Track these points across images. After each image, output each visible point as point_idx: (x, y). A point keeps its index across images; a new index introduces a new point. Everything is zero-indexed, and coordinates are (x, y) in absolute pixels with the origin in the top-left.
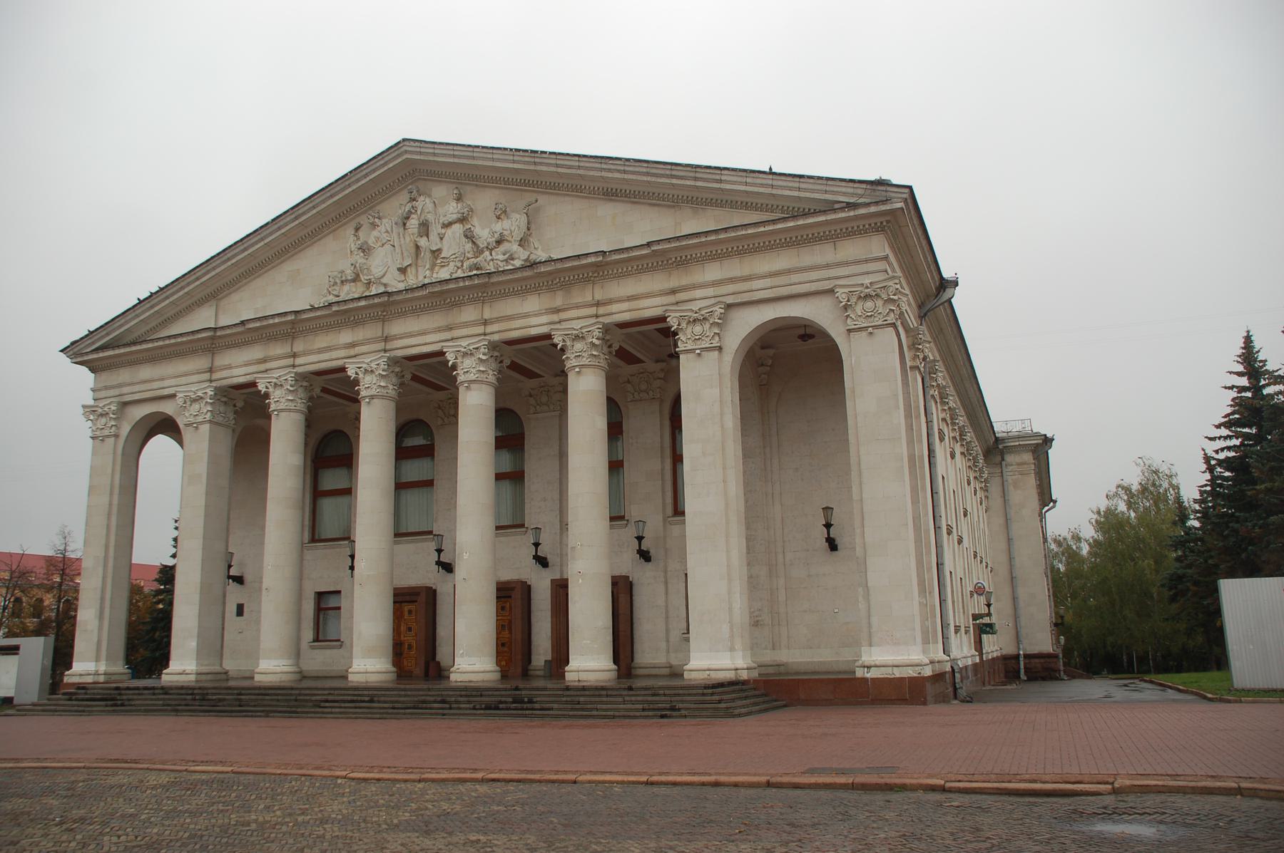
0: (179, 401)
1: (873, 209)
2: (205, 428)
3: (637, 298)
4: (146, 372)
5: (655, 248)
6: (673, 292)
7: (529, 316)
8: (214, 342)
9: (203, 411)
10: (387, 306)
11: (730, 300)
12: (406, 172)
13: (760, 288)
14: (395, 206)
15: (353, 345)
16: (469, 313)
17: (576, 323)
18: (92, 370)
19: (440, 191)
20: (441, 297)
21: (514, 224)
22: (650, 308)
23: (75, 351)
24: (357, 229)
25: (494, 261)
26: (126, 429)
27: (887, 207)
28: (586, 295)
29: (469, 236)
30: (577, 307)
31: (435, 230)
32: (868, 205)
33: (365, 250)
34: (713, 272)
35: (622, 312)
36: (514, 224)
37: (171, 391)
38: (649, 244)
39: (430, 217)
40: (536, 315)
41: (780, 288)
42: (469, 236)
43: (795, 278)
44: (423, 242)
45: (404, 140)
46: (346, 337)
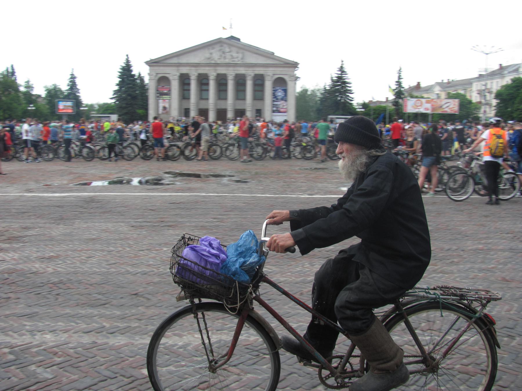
3: (260, 71)
4: (162, 68)
7: (242, 71)
8: (179, 65)
9: (177, 77)
10: (217, 65)
12: (219, 42)
13: (278, 72)
14: (217, 47)
16: (231, 69)
17: (250, 73)
18: (150, 66)
19: (225, 45)
20: (228, 65)
21: (240, 55)
22: (261, 73)
23: (147, 63)
25: (236, 61)
26: (157, 78)
28: (251, 69)
33: (211, 54)
34: (271, 69)
35: (257, 72)
36: (240, 55)
41: (280, 72)
42: (232, 56)
46: (207, 68)
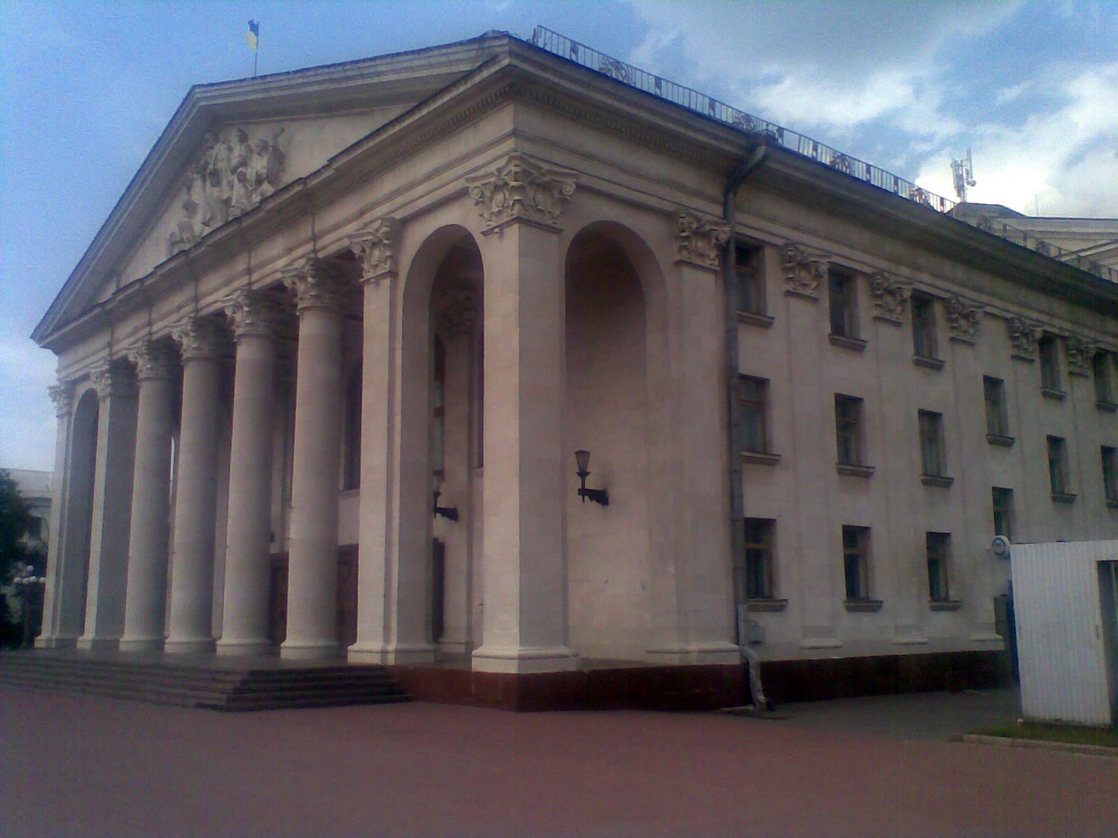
0: (93, 378)
1: (485, 74)
2: (108, 401)
3: (340, 226)
5: (335, 166)
6: (362, 213)
11: (398, 216)
13: (422, 196)
15: (179, 308)
18: (57, 352)
24: (189, 188)
27: (494, 69)
29: (243, 179)
30: (300, 245)
31: (226, 177)
32: (480, 69)
37: (87, 370)
38: (332, 161)
39: (222, 165)
40: (280, 257)
43: (447, 176)
44: (215, 191)
45: (194, 87)
